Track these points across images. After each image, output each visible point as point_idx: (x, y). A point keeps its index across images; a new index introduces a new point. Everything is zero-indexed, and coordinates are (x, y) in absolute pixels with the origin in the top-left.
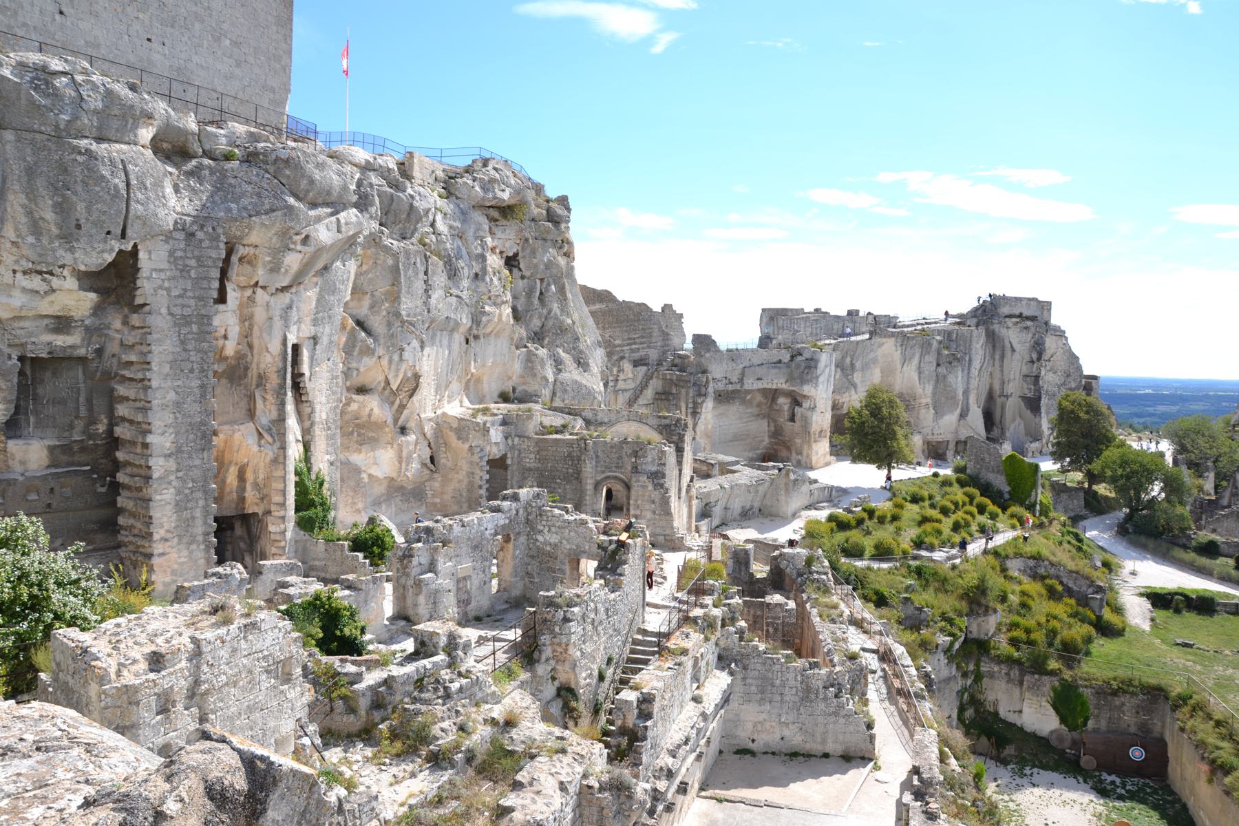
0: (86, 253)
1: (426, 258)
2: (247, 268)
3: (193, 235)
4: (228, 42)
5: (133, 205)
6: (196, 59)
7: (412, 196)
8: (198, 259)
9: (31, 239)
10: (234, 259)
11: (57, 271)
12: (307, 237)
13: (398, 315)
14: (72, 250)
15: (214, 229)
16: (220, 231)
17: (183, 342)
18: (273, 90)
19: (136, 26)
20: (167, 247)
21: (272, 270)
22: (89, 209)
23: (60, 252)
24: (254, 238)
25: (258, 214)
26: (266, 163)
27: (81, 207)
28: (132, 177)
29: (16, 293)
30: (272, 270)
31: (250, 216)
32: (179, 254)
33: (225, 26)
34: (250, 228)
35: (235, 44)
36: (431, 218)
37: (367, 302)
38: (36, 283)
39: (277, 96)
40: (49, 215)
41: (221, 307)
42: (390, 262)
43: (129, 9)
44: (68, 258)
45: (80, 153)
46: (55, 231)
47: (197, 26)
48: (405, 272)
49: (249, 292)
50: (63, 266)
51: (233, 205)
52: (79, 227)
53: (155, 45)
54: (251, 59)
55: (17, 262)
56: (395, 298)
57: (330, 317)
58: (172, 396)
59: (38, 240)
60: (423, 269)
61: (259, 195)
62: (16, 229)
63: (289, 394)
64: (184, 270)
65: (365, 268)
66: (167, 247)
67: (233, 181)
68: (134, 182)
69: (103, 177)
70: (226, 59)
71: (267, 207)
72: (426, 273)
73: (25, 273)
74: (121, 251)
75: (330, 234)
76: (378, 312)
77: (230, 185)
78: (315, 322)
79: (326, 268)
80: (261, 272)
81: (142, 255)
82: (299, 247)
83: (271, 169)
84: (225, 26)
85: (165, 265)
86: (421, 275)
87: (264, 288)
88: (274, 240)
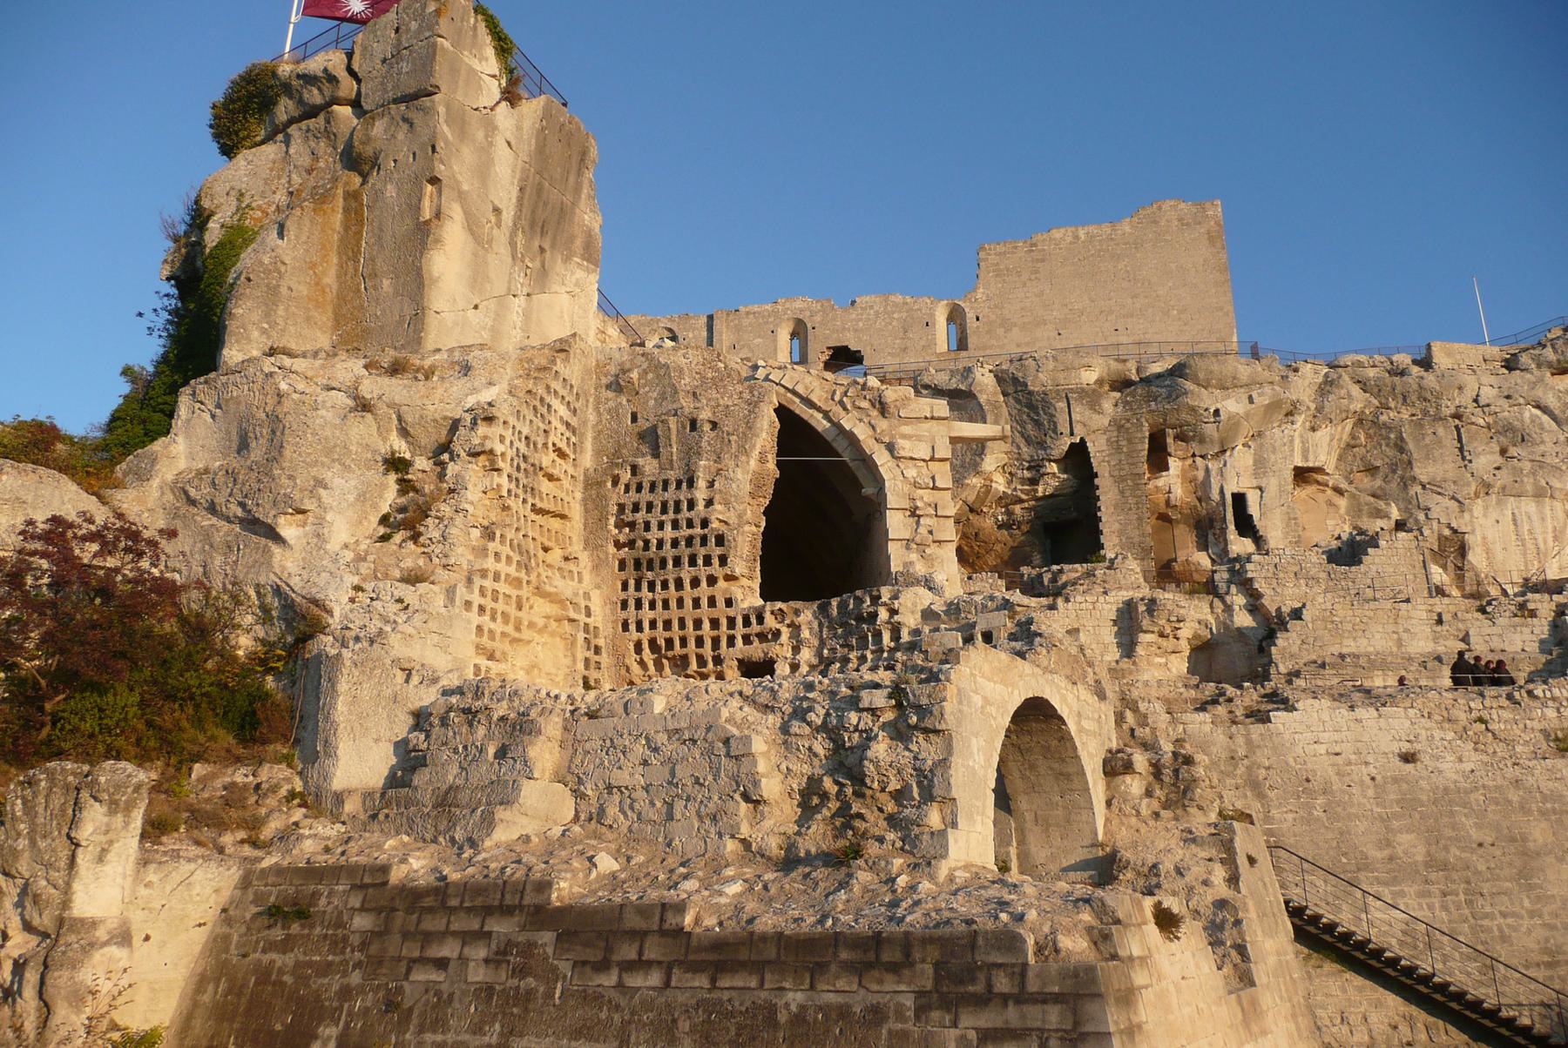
17: (1122, 492)
35: (1180, 312)
49: (1190, 461)
58: (1116, 526)
63: (1232, 527)
64: (1119, 449)
78: (1256, 475)
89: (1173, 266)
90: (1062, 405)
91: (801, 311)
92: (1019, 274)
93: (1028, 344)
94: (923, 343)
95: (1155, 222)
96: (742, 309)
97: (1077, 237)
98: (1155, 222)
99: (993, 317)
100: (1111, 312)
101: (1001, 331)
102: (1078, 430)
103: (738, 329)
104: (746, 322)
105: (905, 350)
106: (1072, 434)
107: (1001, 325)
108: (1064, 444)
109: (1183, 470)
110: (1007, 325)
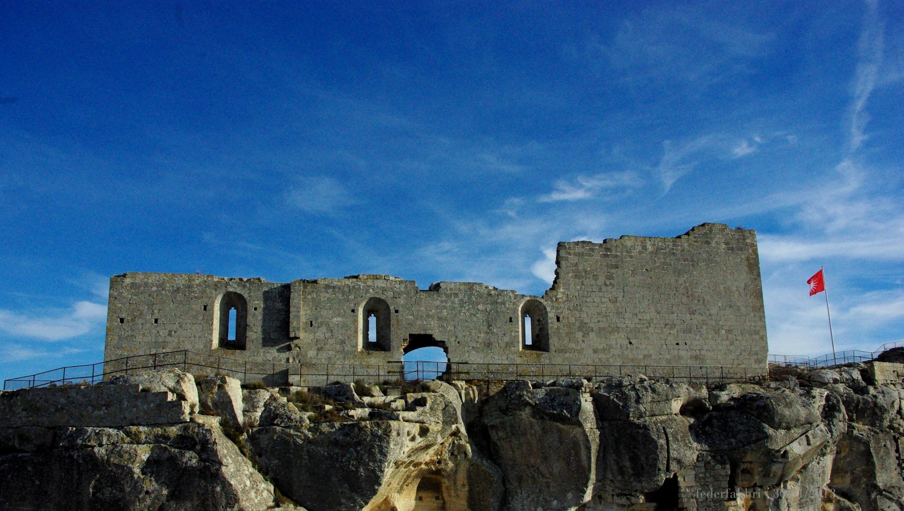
0: (648, 483)
1: (896, 440)
2: (748, 476)
3: (709, 463)
4: (724, 332)
5: (671, 451)
6: (705, 347)
7: (875, 397)
8: (714, 477)
9: (619, 478)
10: (739, 471)
11: (633, 493)
12: (786, 452)
13: (875, 487)
14: (640, 482)
15: (722, 457)
16: (726, 457)
18: (756, 353)
19: (670, 338)
20: (694, 472)
21: (764, 476)
22: (647, 458)
23: (634, 484)
24: (749, 458)
25: (749, 443)
26: (752, 410)
27: (643, 458)
28: (669, 436)
29: (615, 507)
30: (764, 476)
31: (744, 446)
32: (701, 475)
33: (721, 323)
34: (746, 453)
35: (729, 331)
36: (896, 407)
37: (848, 479)
38: (623, 500)
39: (760, 357)
40: (628, 464)
41: (733, 503)
42: (862, 448)
43: (665, 330)
44: (639, 486)
45: (640, 428)
46: (631, 472)
47: (704, 327)
48: (877, 453)
50: (636, 491)
51: (733, 440)
52: (643, 468)
53: (682, 346)
54: (740, 338)
55: (613, 490)
56: (872, 475)
57: (812, 501)
59: (623, 478)
60: (894, 449)
61: (749, 431)
62: (612, 473)
65: (843, 454)
66: (694, 472)
67: (731, 424)
68: (671, 439)
69: (653, 439)
70: (724, 342)
71: (754, 438)
72: (897, 451)
73: (618, 495)
74: (667, 479)
75: (801, 448)
76: (859, 486)
77: (730, 427)
79: (805, 467)
80: (757, 478)
81: (680, 479)
82: (780, 460)
83: (755, 413)
84: (721, 323)
85: (694, 484)
86: (893, 454)
87: (761, 487)
88: (762, 457)
89: (722, 287)
90: (662, 441)
91: (384, 290)
92: (596, 277)
93: (604, 350)
94: (506, 339)
95: (708, 243)
96: (322, 283)
97: (644, 248)
98: (708, 243)
99: (572, 320)
100: (673, 326)
101: (579, 335)
102: (674, 466)
103: (317, 304)
104: (324, 296)
105: (489, 345)
106: (668, 469)
107: (580, 329)
108: (663, 477)
109: (746, 500)
110: (583, 327)
